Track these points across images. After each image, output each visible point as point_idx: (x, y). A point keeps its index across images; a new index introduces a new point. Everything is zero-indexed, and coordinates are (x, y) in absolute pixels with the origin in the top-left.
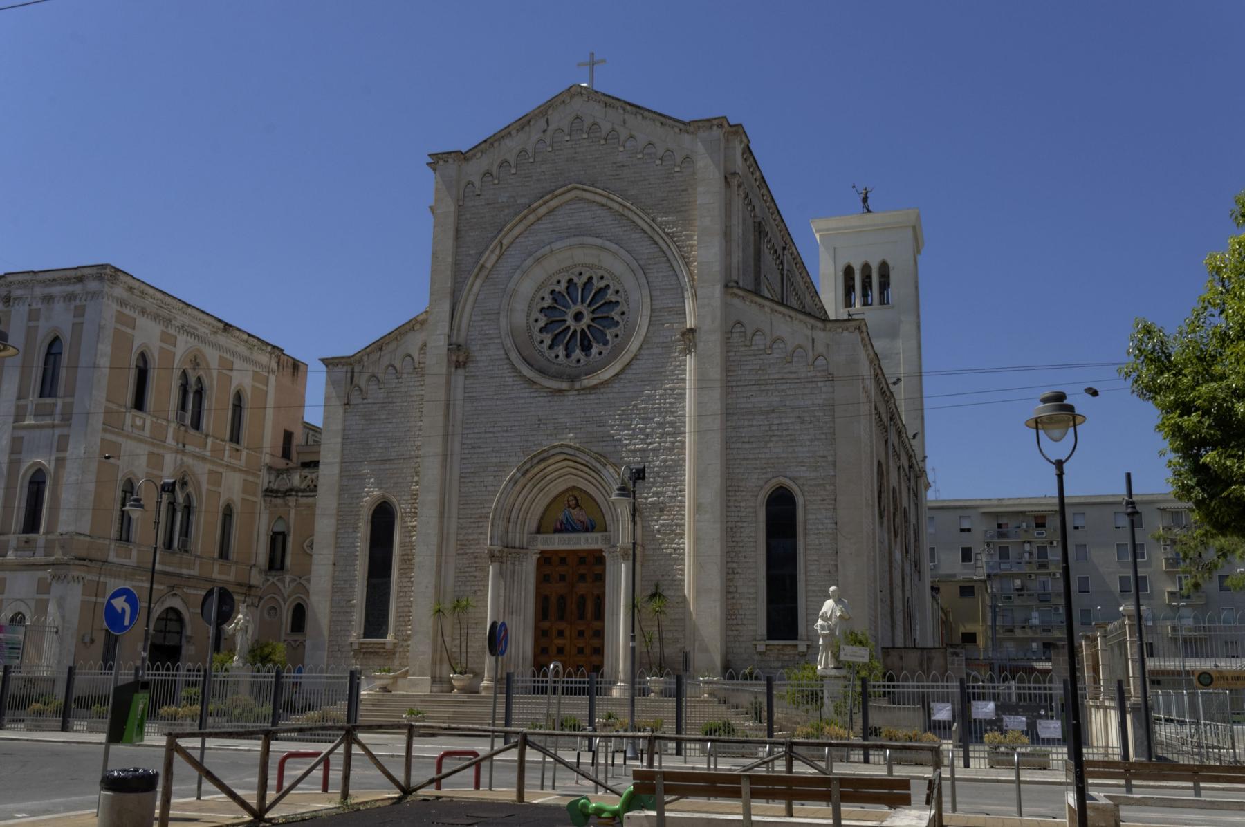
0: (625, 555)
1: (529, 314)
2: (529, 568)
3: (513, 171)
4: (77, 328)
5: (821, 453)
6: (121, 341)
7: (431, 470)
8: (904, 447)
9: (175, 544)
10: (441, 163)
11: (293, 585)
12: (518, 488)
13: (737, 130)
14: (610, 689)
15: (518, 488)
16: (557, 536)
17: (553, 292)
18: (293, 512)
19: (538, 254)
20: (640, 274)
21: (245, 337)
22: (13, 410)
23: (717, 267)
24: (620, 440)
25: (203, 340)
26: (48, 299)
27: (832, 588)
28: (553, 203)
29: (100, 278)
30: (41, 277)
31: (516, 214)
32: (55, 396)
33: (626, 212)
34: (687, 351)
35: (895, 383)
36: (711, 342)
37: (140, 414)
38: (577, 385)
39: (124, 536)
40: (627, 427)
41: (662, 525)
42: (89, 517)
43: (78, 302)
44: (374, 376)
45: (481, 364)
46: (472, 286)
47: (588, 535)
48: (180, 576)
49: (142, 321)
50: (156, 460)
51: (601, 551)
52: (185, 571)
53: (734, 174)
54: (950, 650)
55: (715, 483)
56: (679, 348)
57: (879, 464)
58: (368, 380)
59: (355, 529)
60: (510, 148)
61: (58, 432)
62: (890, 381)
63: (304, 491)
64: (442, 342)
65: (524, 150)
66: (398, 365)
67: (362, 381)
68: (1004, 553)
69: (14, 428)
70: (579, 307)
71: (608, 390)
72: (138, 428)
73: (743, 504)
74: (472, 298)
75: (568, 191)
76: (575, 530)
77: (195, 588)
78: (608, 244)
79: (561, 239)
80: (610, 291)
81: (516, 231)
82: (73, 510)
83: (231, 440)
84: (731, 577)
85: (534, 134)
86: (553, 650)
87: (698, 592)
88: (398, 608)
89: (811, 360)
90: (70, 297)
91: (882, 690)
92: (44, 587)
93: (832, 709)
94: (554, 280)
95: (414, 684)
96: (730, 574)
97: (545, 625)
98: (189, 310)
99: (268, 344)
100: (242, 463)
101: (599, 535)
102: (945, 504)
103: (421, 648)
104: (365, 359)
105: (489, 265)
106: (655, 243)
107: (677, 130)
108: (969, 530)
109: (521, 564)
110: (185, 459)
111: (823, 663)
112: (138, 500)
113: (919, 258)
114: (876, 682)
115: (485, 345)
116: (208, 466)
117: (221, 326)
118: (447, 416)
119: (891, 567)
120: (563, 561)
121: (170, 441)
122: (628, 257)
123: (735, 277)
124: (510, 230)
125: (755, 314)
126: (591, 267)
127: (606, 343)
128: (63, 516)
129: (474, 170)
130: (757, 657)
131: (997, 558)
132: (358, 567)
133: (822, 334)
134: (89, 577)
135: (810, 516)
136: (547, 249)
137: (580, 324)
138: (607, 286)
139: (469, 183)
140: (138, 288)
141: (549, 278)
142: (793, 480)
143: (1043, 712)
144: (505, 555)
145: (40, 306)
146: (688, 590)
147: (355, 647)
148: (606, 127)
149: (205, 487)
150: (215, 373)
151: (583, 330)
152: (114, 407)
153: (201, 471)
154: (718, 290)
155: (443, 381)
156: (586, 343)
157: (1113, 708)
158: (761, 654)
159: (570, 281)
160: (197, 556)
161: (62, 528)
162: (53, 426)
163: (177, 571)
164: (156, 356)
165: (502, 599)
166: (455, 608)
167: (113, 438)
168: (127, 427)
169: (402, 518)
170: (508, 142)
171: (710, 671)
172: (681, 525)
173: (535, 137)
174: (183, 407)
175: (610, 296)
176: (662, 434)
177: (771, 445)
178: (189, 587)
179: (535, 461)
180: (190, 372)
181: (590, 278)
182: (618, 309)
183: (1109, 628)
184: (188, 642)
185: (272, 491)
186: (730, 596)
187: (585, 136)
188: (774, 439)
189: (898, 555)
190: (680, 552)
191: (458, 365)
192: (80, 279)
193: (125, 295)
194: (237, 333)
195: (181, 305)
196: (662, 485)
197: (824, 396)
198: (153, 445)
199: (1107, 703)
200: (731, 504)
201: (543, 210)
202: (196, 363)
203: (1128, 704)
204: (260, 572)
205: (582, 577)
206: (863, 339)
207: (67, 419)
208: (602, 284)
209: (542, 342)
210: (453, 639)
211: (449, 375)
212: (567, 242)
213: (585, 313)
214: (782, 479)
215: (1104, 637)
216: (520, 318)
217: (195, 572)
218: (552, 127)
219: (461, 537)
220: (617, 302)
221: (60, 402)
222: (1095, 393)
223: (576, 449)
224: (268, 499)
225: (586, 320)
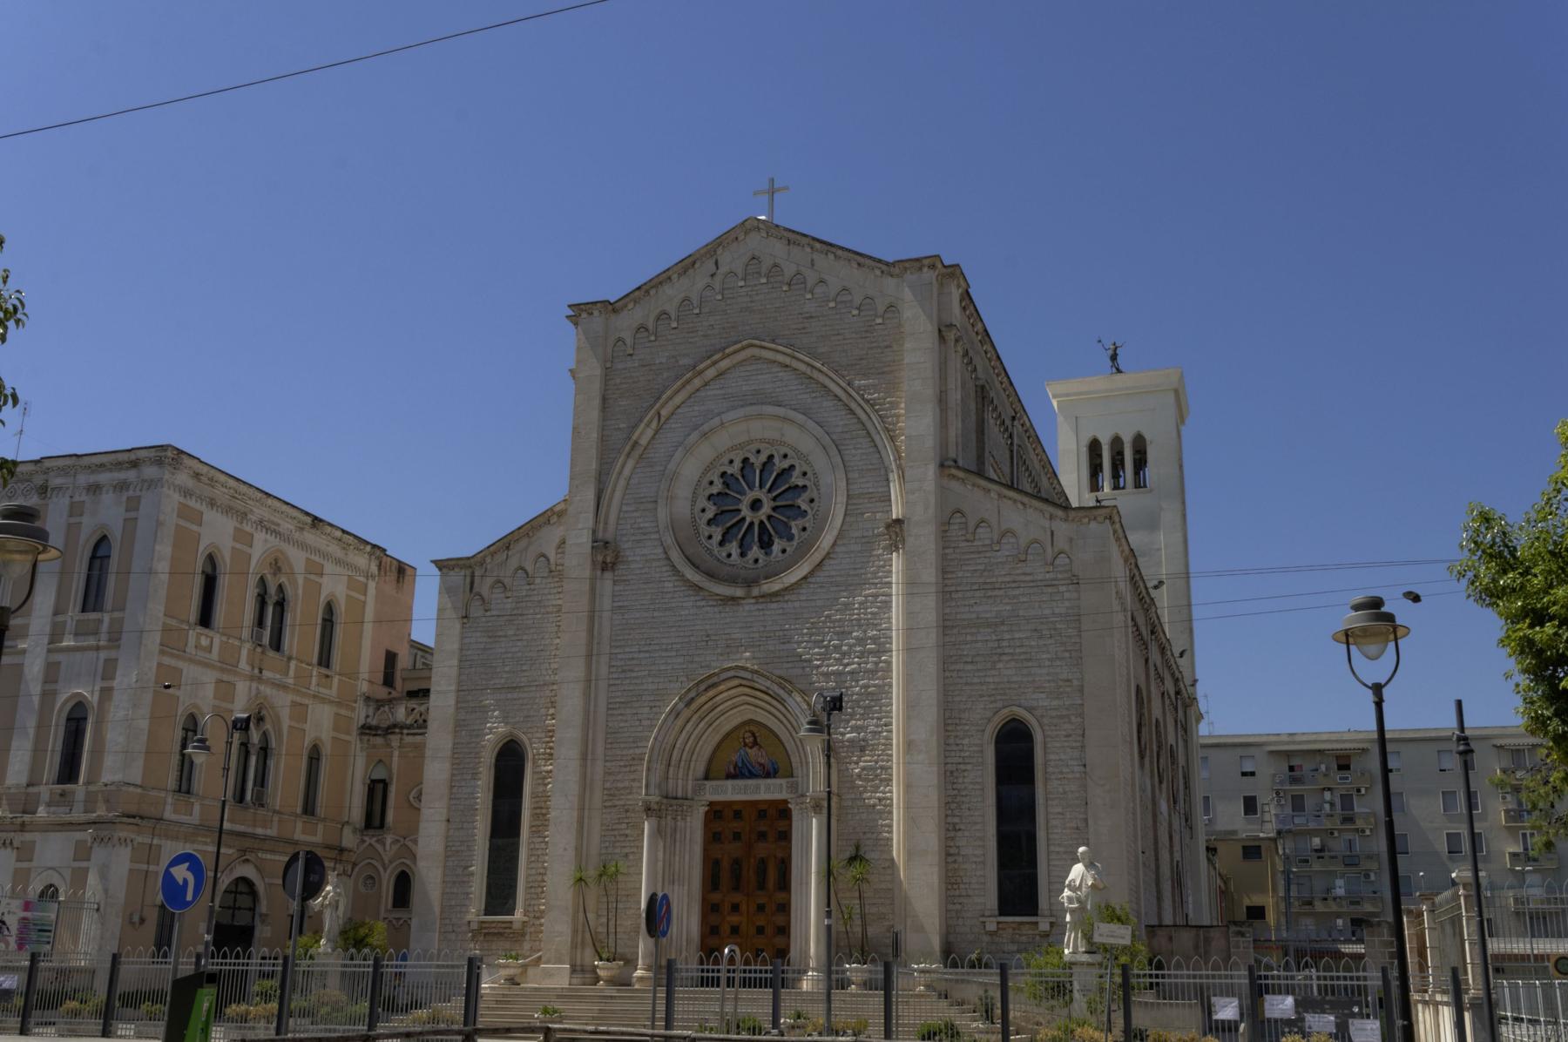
0: (817, 808)
1: (694, 502)
2: (694, 826)
3: (674, 325)
4: (130, 524)
5: (1064, 676)
7: (571, 701)
8: (1169, 667)
10: (584, 315)
11: (395, 847)
12: (680, 722)
13: (954, 272)
14: (800, 980)
15: (680, 722)
16: (730, 783)
17: (723, 474)
18: (396, 753)
19: (706, 427)
20: (833, 451)
21: (339, 534)
22: (48, 629)
23: (930, 442)
24: (810, 661)
25: (288, 540)
26: (95, 489)
27: (1082, 849)
28: (724, 364)
29: (159, 462)
30: (86, 461)
31: (677, 378)
32: (101, 610)
33: (816, 375)
35: (1156, 587)
36: (924, 536)
37: (206, 631)
38: (755, 591)
39: (184, 786)
40: (818, 644)
41: (863, 769)
42: (140, 763)
43: (131, 493)
45: (633, 566)
47: (769, 781)
48: (254, 836)
49: (210, 515)
51: (786, 802)
52: (259, 831)
53: (951, 326)
54: (1233, 928)
55: (931, 714)
56: (883, 544)
58: (492, 587)
59: (475, 777)
60: (670, 296)
61: (103, 655)
62: (1150, 584)
63: (409, 727)
64: (585, 539)
66: (529, 569)
67: (484, 587)
68: (1298, 803)
69: (49, 651)
70: (756, 493)
71: (793, 597)
73: (966, 741)
74: (622, 482)
75: (743, 348)
76: (752, 775)
77: (273, 852)
78: (792, 414)
79: (734, 408)
80: (796, 473)
81: (678, 399)
82: (121, 753)
83: (320, 664)
84: (952, 834)
85: (697, 282)
86: (726, 929)
87: (910, 854)
88: (528, 876)
90: (122, 486)
92: (82, 853)
93: (1085, 1006)
94: (725, 460)
95: (548, 974)
96: (950, 830)
97: (716, 897)
98: (270, 501)
100: (333, 692)
101: (783, 781)
102: (1222, 741)
103: (557, 929)
104: (488, 560)
105: (644, 442)
106: (852, 412)
107: (878, 272)
108: (1253, 774)
109: (684, 819)
110: (262, 688)
112: (202, 741)
113: (1183, 428)
115: (639, 541)
117: (309, 520)
118: (591, 631)
119: (1155, 822)
120: (738, 815)
121: (243, 665)
122: (819, 431)
123: (952, 454)
124: (670, 398)
125: (982, 501)
126: (771, 443)
127: (791, 538)
128: (108, 761)
130: (986, 938)
131: (1288, 810)
132: (478, 824)
133: (1064, 526)
134: (140, 839)
135: (1052, 757)
136: (716, 421)
137: (758, 515)
138: (792, 467)
139: (619, 339)
140: (207, 475)
141: (719, 457)
142: (1030, 710)
143: (1356, 1010)
144: (665, 808)
146: (897, 852)
147: (474, 926)
148: (789, 270)
149: (286, 723)
150: (300, 581)
151: (762, 522)
152: (174, 622)
153: (282, 702)
154: (931, 471)
155: (586, 587)
156: (766, 538)
157: (1446, 1004)
158: (991, 934)
159: (746, 460)
160: (275, 812)
161: (106, 777)
162: (98, 648)
163: (250, 830)
164: (228, 560)
165: (660, 864)
166: (601, 876)
168: (190, 649)
170: (668, 290)
171: (926, 956)
172: (887, 769)
173: (701, 281)
174: (260, 622)
175: (796, 479)
176: (862, 653)
177: (1000, 665)
179: (703, 687)
180: (269, 577)
181: (771, 457)
182: (806, 495)
183: (1438, 899)
184: (263, 922)
185: (370, 728)
186: (950, 859)
187: (764, 280)
188: (1005, 658)
189: (1163, 806)
190: (886, 803)
191: (605, 567)
192: (135, 464)
193: (190, 483)
194: (329, 529)
195: (260, 495)
196: (864, 717)
197: (1067, 604)
198: (222, 670)
199: (1438, 998)
200: (951, 741)
201: (711, 373)
202: (277, 570)
203: (1466, 999)
204: (355, 831)
205: (762, 836)
206: (1115, 532)
207: (115, 639)
208: (785, 464)
209: (710, 537)
210: (599, 916)
211: (593, 580)
212: (741, 412)
213: (765, 500)
214: (1015, 709)
215: (1431, 911)
216: (682, 508)
217: (272, 832)
219: (608, 785)
220: (805, 487)
221: (106, 618)
222: (1416, 598)
223: (756, 672)
225: (766, 509)
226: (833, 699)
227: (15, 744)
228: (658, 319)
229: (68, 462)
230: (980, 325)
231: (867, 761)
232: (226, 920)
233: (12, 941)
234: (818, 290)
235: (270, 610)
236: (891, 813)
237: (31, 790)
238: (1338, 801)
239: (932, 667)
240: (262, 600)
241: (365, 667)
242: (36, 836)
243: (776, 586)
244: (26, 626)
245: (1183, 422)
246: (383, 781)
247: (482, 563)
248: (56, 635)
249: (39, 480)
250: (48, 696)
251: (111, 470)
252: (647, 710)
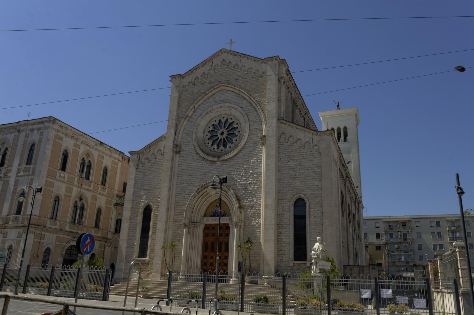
1: (204, 133)
2: (200, 231)
3: (200, 81)
5: (316, 184)
7: (164, 192)
8: (353, 190)
10: (174, 79)
12: (196, 199)
13: (283, 62)
14: (230, 280)
15: (196, 199)
16: (211, 218)
17: (213, 125)
19: (208, 110)
21: (109, 147)
22: (16, 170)
23: (274, 112)
24: (237, 180)
25: (92, 148)
27: (318, 238)
28: (214, 92)
29: (49, 121)
30: (30, 122)
31: (200, 96)
33: (241, 93)
34: (263, 144)
35: (348, 163)
36: (272, 141)
37: (63, 172)
38: (221, 159)
39: (54, 217)
40: (239, 175)
41: (252, 214)
43: (41, 131)
44: (147, 158)
45: (185, 152)
46: (183, 123)
50: (69, 190)
51: (228, 224)
53: (282, 78)
54: (371, 267)
55: (273, 196)
56: (260, 144)
57: (342, 192)
59: (137, 216)
60: (199, 73)
61: (30, 177)
62: (346, 162)
64: (171, 144)
65: (204, 73)
66: (156, 154)
68: (391, 235)
69: (16, 176)
70: (223, 130)
71: (232, 161)
72: (62, 177)
73: (284, 205)
74: (183, 127)
75: (220, 87)
79: (217, 104)
80: (234, 124)
81: (200, 102)
83: (102, 184)
84: (279, 234)
85: (208, 67)
86: (209, 264)
87: (265, 240)
89: (312, 147)
90: (39, 129)
91: (339, 282)
93: (318, 291)
94: (214, 120)
95: (154, 276)
96: (279, 233)
97: (206, 254)
98: (86, 136)
99: (118, 151)
100: (106, 193)
101: (227, 218)
103: (158, 262)
104: (144, 151)
105: (189, 115)
107: (260, 62)
108: (379, 227)
110: (82, 190)
111: (314, 271)
113: (358, 126)
114: (336, 280)
116: (91, 193)
118: (171, 172)
119: (347, 234)
120: (214, 228)
121: (75, 183)
123: (282, 116)
124: (198, 102)
125: (290, 129)
126: (227, 115)
127: (232, 143)
129: (186, 81)
130: (290, 268)
131: (389, 237)
132: (137, 230)
133: (316, 137)
134: (38, 232)
136: (211, 108)
137: (223, 136)
138: (234, 122)
140: (64, 126)
143: (416, 295)
145: (29, 133)
146: (262, 240)
148: (234, 63)
149: (90, 201)
150: (96, 160)
151: (224, 139)
153: (89, 195)
154: (275, 121)
155: (170, 158)
156: (225, 144)
157: (451, 293)
158: (291, 267)
159: (220, 120)
160: (85, 226)
162: (29, 175)
163: (76, 231)
164: (71, 152)
165: (189, 243)
166: (171, 247)
167: (51, 180)
168: (57, 177)
169: (154, 211)
170: (198, 71)
171: (269, 274)
173: (208, 68)
175: (235, 125)
177: (296, 181)
179: (203, 188)
181: (227, 119)
182: (237, 130)
183: (443, 256)
186: (279, 243)
187: (226, 66)
188: (297, 179)
189: (351, 230)
190: (259, 224)
191: (177, 152)
192: (43, 122)
193: (59, 128)
194: (106, 146)
195: (82, 134)
196: (252, 197)
197: (317, 161)
198: (68, 184)
199: (443, 290)
200: (280, 205)
201: (210, 94)
202: (88, 155)
203: (460, 292)
204: (112, 233)
205: (221, 235)
206: (333, 140)
207: (33, 173)
208: (232, 121)
210: (170, 259)
212: (218, 106)
213: (225, 132)
214: (300, 195)
215: (441, 260)
216: (200, 135)
218: (215, 64)
219: (175, 218)
220: (237, 128)
221: (32, 166)
222: (462, 69)
226: (223, 179)
227: (5, 203)
228: (195, 79)
229: (26, 122)
230: (293, 82)
231: (253, 211)
232: (67, 258)
234: (242, 69)
235: (85, 168)
236: (260, 227)
237: (8, 217)
238: (402, 235)
239: (273, 181)
240: (83, 164)
241: (117, 187)
243: (227, 157)
244: (11, 170)
245: (358, 124)
247: (142, 153)
248: (18, 173)
249: (18, 128)
250: (15, 189)
252: (187, 196)
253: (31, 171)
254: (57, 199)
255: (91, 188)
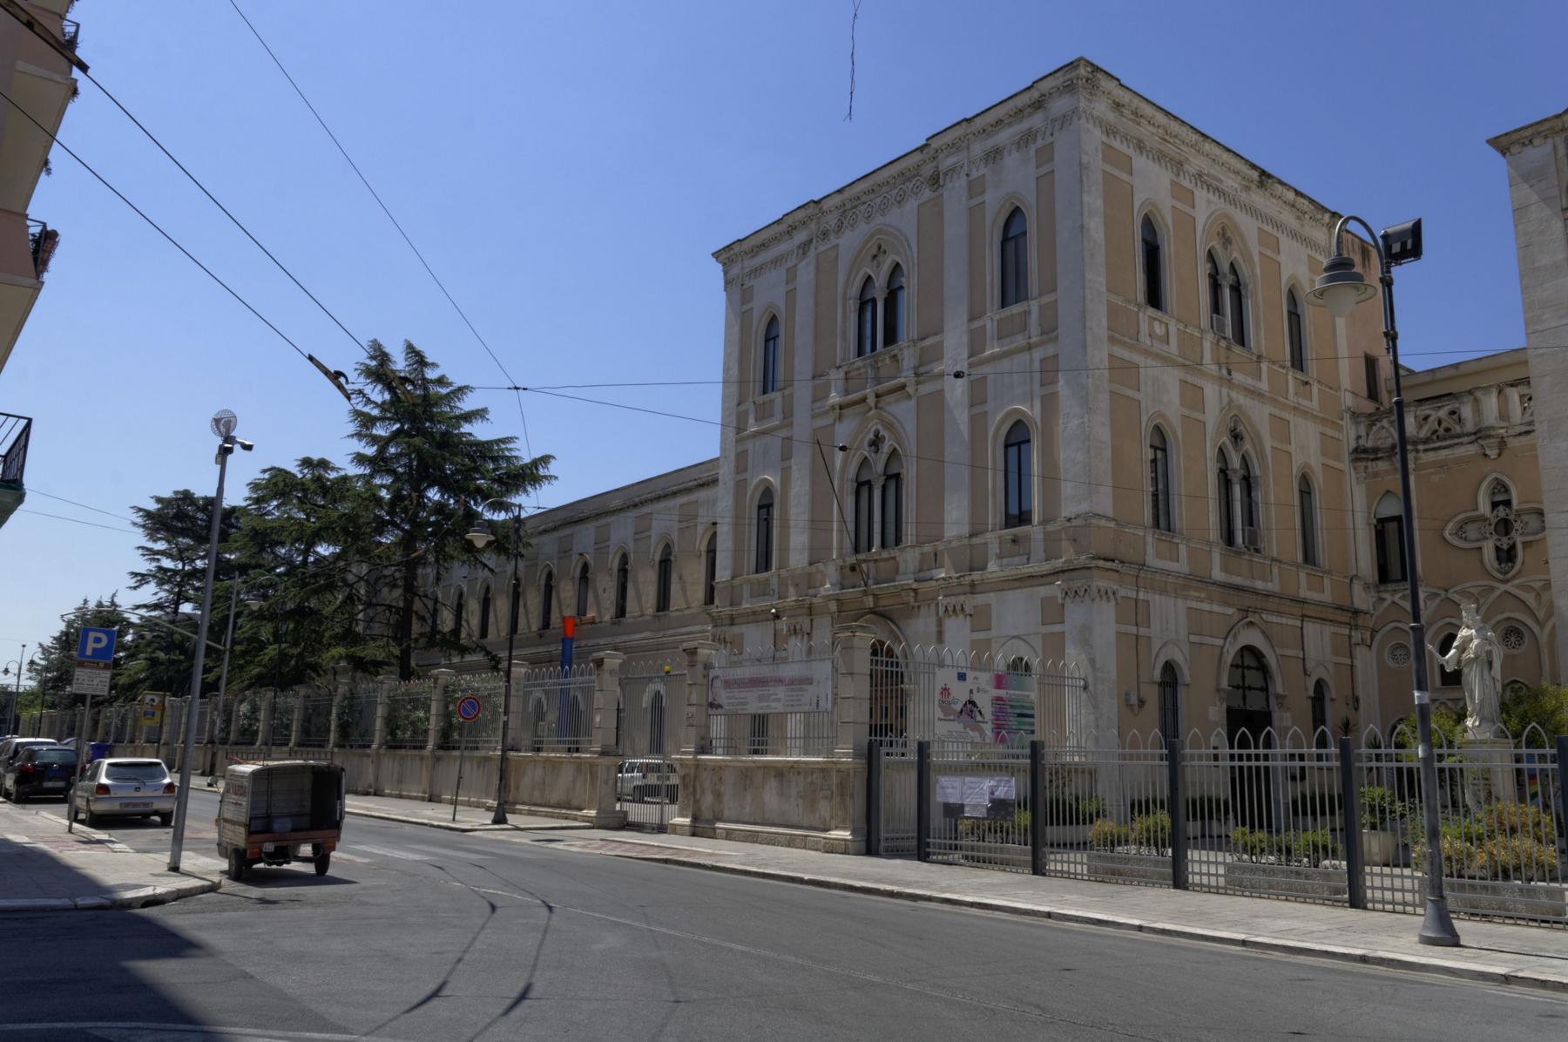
4: (1046, 182)
6: (1118, 194)
9: (1239, 538)
11: (1433, 604)
21: (1291, 195)
22: (965, 339)
29: (1070, 88)
30: (979, 123)
32: (1026, 298)
37: (1158, 314)
43: (1040, 143)
48: (1255, 592)
49: (1141, 162)
52: (1259, 585)
61: (1038, 354)
63: (1426, 441)
77: (1279, 613)
82: (1083, 474)
83: (1293, 366)
90: (1028, 138)
92: (1053, 613)
98: (1207, 147)
99: (1324, 209)
110: (1234, 395)
116: (1267, 409)
128: (1067, 489)
140: (1133, 107)
149: (1268, 443)
150: (1256, 258)
152: (1119, 301)
153: (1259, 415)
161: (1068, 510)
162: (1030, 347)
163: (1248, 583)
168: (1145, 339)
174: (1216, 307)
178: (1272, 612)
184: (1281, 705)
185: (1365, 451)
192: (1039, 105)
193: (1111, 117)
195: (1195, 137)
204: (1367, 587)
207: (1049, 331)
217: (1273, 586)
221: (1034, 306)
224: (1362, 465)
229: (958, 132)
232: (1237, 703)
233: (988, 728)
235: (1227, 293)
237: (975, 540)
241: (1345, 382)
242: (991, 598)
246: (1398, 519)
248: (975, 346)
251: (1010, 124)
253: (1034, 328)
254: (1160, 442)
255: (1264, 386)
